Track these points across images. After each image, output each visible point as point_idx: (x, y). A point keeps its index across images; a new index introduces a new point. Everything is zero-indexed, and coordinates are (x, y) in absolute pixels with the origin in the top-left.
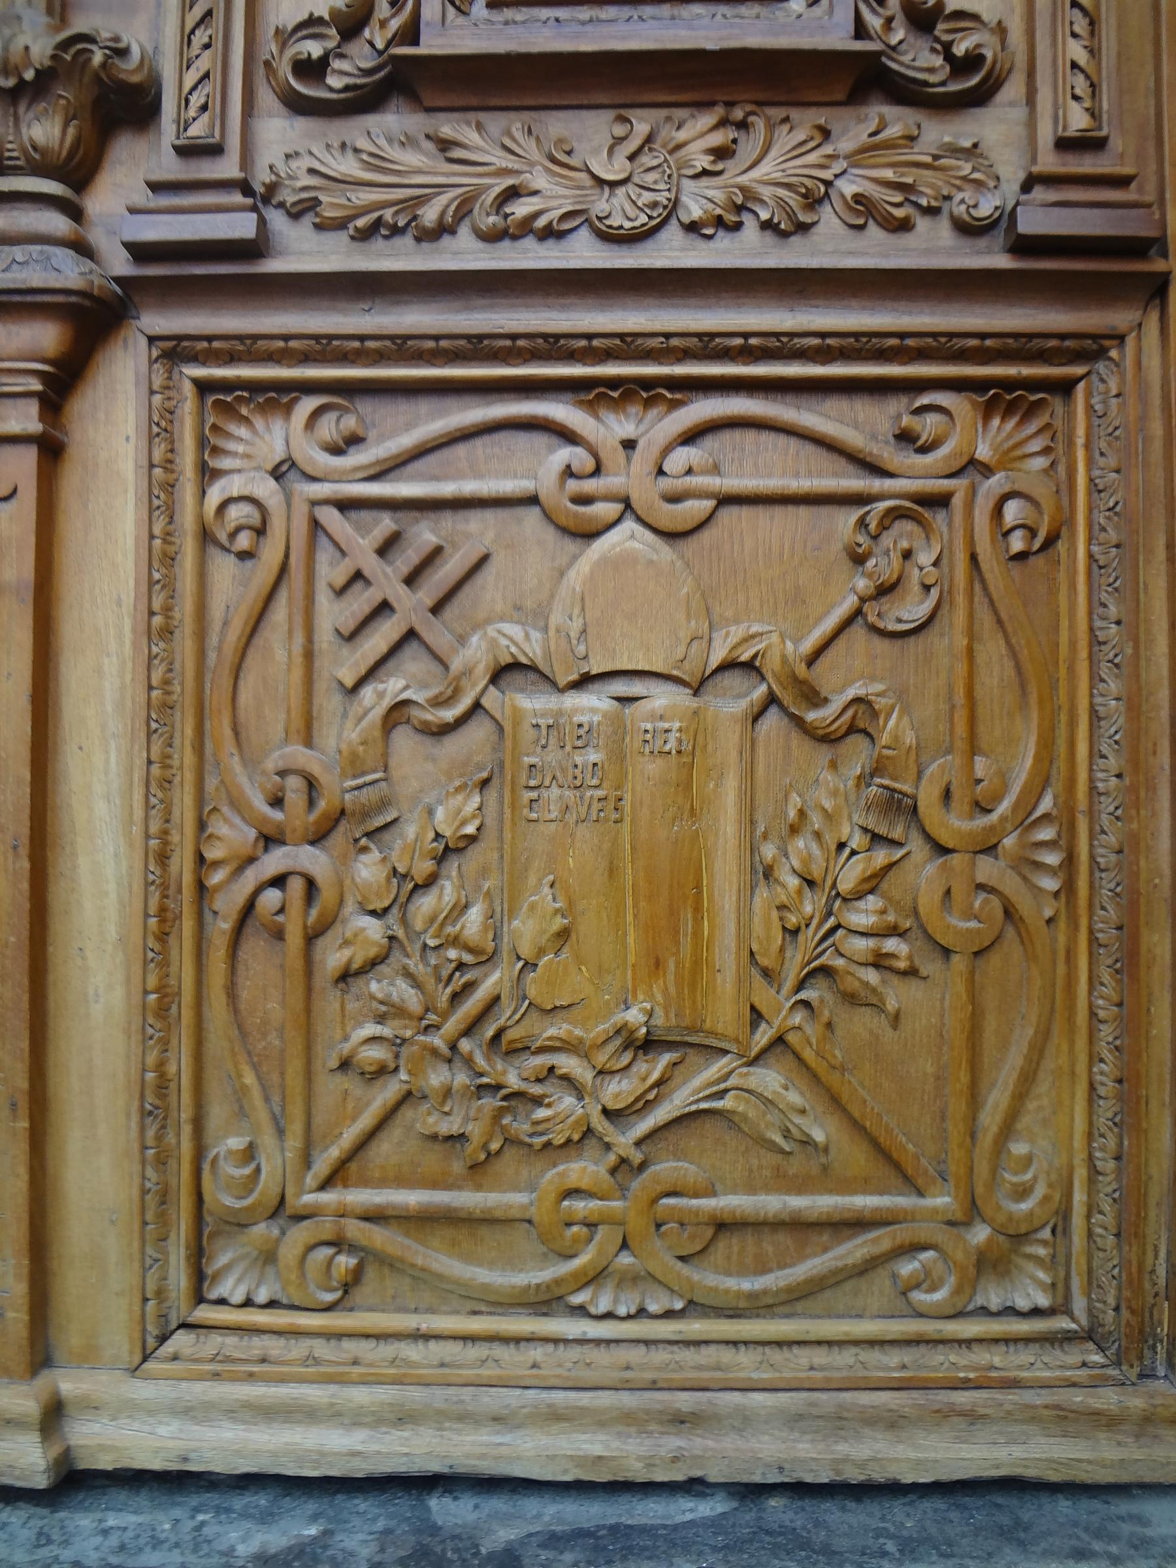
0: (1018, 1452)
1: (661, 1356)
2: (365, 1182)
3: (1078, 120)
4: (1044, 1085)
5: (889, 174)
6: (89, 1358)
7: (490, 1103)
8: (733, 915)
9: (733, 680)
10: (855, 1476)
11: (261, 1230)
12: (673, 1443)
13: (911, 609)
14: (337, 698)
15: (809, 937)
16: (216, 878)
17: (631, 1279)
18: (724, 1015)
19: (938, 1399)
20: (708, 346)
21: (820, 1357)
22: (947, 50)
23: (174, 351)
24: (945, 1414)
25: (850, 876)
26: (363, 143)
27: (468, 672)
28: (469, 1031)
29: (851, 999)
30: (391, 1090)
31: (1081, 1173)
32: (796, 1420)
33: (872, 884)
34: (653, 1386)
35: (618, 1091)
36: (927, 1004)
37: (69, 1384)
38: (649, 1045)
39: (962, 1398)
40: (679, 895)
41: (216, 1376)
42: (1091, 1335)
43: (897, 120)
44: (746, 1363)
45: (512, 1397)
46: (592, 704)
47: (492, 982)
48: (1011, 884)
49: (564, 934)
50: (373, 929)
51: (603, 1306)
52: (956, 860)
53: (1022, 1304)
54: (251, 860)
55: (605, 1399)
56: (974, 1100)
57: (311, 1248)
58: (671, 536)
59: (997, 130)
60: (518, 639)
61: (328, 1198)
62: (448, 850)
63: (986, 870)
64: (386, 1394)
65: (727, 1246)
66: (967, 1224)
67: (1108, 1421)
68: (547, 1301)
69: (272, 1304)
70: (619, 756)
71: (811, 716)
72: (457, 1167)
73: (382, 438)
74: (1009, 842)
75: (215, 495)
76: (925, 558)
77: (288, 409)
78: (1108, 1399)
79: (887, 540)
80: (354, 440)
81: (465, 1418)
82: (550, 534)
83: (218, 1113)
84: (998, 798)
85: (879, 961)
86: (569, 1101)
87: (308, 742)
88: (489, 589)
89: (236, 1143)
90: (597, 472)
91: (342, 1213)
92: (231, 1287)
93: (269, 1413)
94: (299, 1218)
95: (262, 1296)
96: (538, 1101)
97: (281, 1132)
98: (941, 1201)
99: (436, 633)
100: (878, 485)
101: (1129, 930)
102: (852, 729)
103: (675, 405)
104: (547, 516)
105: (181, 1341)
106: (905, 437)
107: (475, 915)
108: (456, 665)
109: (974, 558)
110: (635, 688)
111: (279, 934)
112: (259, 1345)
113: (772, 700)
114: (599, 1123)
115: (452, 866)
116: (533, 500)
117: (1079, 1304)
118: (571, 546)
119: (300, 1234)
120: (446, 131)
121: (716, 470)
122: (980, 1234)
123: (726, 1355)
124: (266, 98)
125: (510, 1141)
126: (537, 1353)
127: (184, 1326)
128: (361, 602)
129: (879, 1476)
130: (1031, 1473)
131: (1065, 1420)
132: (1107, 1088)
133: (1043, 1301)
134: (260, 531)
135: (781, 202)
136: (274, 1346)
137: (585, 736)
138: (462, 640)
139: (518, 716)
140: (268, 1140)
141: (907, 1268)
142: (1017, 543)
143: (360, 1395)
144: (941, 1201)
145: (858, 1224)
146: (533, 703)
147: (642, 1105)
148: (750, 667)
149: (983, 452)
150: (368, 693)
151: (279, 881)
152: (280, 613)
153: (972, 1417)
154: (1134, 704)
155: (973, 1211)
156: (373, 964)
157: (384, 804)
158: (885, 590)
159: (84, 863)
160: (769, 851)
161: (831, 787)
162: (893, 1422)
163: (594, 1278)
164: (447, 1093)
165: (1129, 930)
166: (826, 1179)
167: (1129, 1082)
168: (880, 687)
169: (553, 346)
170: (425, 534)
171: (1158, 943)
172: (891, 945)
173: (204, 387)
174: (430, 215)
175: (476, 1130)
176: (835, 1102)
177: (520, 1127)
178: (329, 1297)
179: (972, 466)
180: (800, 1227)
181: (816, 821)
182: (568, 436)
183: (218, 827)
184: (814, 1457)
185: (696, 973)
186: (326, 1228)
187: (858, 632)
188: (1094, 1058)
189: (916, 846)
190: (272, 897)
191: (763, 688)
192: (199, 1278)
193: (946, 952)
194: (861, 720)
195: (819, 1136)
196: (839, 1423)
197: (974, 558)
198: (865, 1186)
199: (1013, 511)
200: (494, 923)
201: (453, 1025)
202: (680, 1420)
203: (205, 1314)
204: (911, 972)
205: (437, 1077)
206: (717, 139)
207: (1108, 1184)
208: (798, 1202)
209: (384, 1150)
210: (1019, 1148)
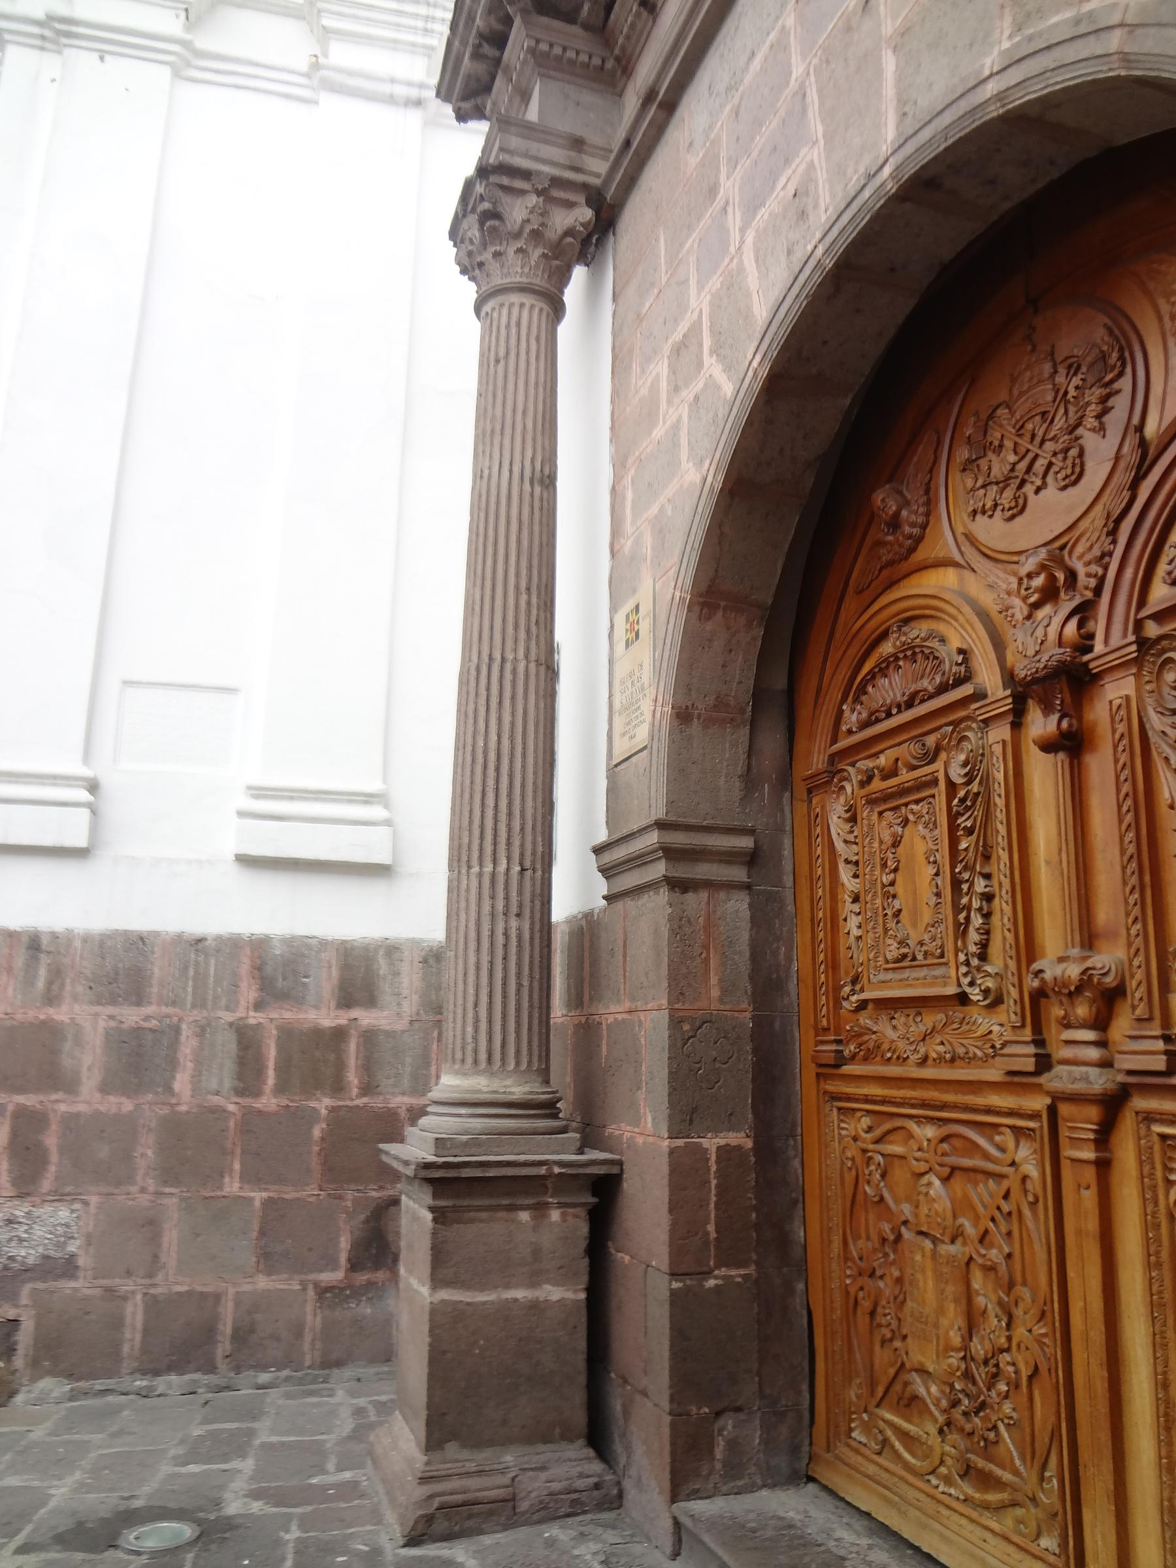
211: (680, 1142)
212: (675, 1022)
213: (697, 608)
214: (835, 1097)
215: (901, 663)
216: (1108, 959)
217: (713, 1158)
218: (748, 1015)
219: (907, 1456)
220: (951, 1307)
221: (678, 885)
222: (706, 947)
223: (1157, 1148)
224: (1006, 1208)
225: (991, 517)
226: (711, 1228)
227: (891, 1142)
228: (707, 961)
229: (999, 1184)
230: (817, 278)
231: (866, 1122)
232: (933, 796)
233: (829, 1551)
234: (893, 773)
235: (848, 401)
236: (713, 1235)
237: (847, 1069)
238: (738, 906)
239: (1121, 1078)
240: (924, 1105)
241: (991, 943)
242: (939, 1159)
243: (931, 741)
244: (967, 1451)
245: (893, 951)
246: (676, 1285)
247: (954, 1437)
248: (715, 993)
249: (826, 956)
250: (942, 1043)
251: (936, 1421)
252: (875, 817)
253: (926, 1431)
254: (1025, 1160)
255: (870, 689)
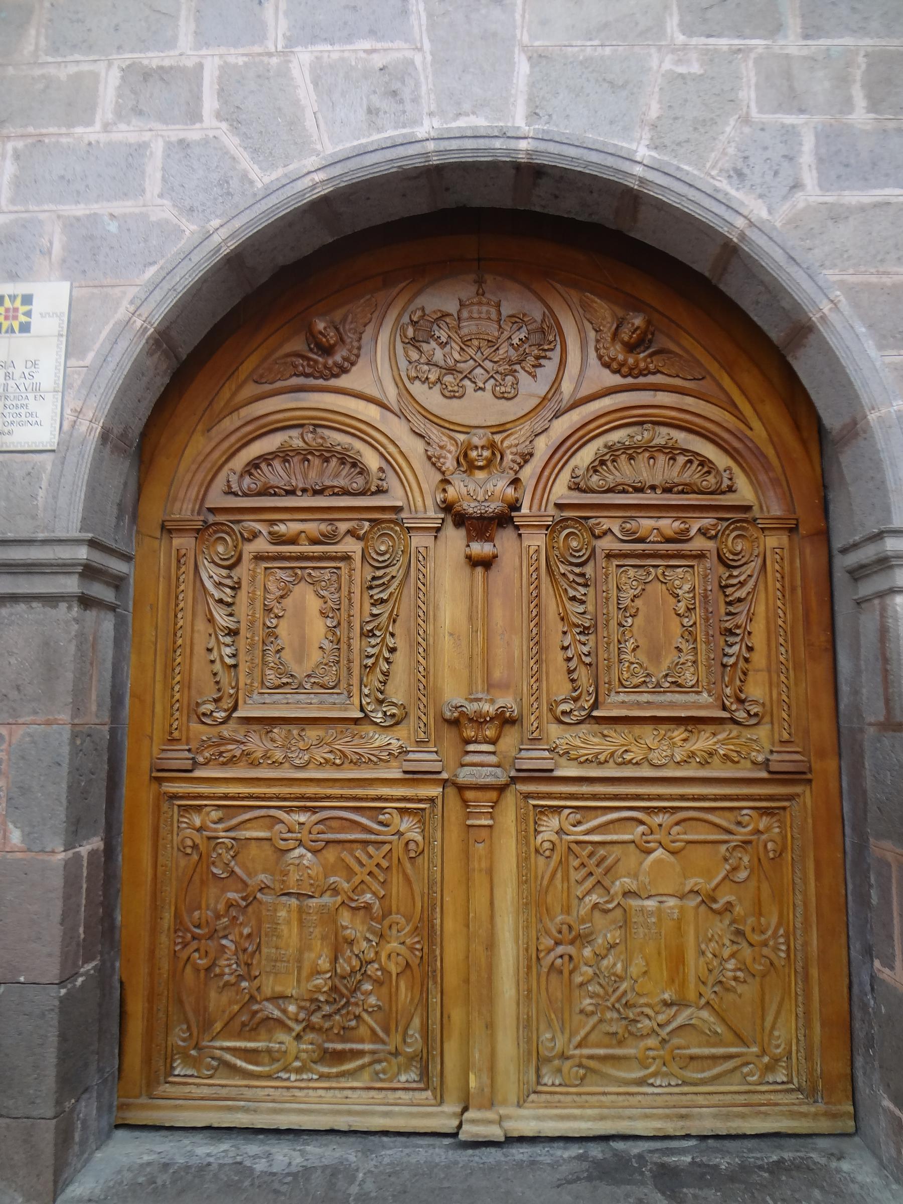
0: (779, 1124)
1: (675, 1098)
2: (587, 1047)
3: (786, 736)
4: (783, 1013)
5: (732, 747)
6: (504, 1103)
7: (624, 1022)
8: (693, 965)
9: (692, 895)
10: (733, 1132)
11: (556, 1062)
12: (681, 1123)
13: (742, 875)
14: (577, 901)
15: (716, 972)
16: (542, 955)
17: (666, 1075)
18: (692, 995)
19: (755, 1109)
20: (683, 798)
21: (721, 1097)
22: (748, 712)
23: (527, 796)
24: (759, 1113)
25: (726, 953)
26: (581, 735)
27: (616, 893)
28: (619, 1000)
29: (727, 990)
30: (595, 1019)
31: (794, 1041)
32: (715, 1116)
33: (733, 955)
34: (674, 1107)
35: (661, 1018)
36: (748, 991)
37: (502, 1111)
38: (667, 1004)
39: (763, 1109)
40: (677, 960)
41: (546, 1107)
42: (799, 1090)
43: (735, 731)
44: (700, 1100)
45: (634, 1111)
46: (651, 904)
47: (624, 986)
48: (773, 956)
49: (645, 973)
50: (590, 971)
51: (658, 1083)
52: (756, 949)
53: (779, 1080)
54: (553, 950)
55: (660, 1111)
56: (763, 1019)
57: (571, 1067)
58: (673, 853)
59: (762, 732)
60: (627, 882)
61: (577, 1052)
62: (612, 946)
63: (765, 951)
64: (596, 1111)
65: (694, 1064)
66: (762, 1056)
67: (804, 1115)
68: (641, 1082)
69: (560, 1085)
70: (660, 919)
71: (715, 906)
72: (614, 1042)
73: (587, 822)
74: (771, 943)
75: (539, 838)
76: (746, 859)
77: (560, 813)
78: (804, 1109)
79: (735, 854)
80: (579, 823)
81: (620, 1117)
82: (638, 852)
83: (542, 1026)
84: (767, 930)
85: (735, 979)
86: (647, 1022)
87: (568, 914)
88: (621, 868)
89: (548, 1036)
90: (652, 833)
91: (581, 1056)
92: (547, 1079)
93: (562, 1118)
94: (568, 1058)
95: (557, 1082)
96: (638, 1021)
97: (562, 1033)
98: (755, 1049)
99: (606, 882)
100: (731, 837)
101: (806, 968)
102: (726, 910)
103: (673, 814)
104: (637, 846)
105: (533, 1097)
106: (739, 823)
107: (619, 966)
108: (612, 892)
109: (759, 860)
110: (664, 898)
111: (561, 972)
112: (557, 1097)
113: (703, 901)
114: (656, 1027)
115: (612, 951)
116: (633, 842)
117: (795, 1080)
118: (644, 855)
119: (568, 1064)
120: (605, 732)
121: (685, 833)
122: (766, 1059)
123: (694, 1097)
124: (550, 715)
125: (631, 1034)
126: (639, 1098)
127: (535, 1092)
128: (583, 872)
129: (740, 1132)
130: (783, 1131)
131: (793, 1115)
132: (801, 1015)
133: (785, 1079)
134: (552, 850)
135: (703, 756)
136: (562, 1098)
137: (651, 914)
138: (613, 883)
139: (630, 906)
140: (559, 1034)
141: (745, 1070)
142: (771, 855)
143: (589, 1112)
144: (755, 1049)
145: (730, 1057)
146: (634, 903)
147: (669, 1022)
148: (697, 892)
149: (761, 827)
150: (587, 899)
151: (561, 957)
152: (559, 875)
153: (766, 1114)
154: (805, 904)
155: (764, 1052)
156: (589, 981)
157: (592, 933)
158: (735, 869)
159: (502, 951)
160: (703, 946)
161: (720, 927)
162: (743, 1116)
163: (655, 1075)
164: (612, 1020)
165: (806, 968)
166: (721, 1044)
167: (807, 1013)
168: (734, 898)
169: (638, 797)
170: (602, 852)
171: (814, 972)
172: (739, 974)
173: (534, 806)
174: (602, 758)
175: (620, 1031)
176: (723, 1020)
177: (633, 1029)
178: (578, 1082)
179: (758, 832)
180: (714, 1058)
181: (716, 937)
182: (642, 823)
183: (542, 940)
184: (722, 1127)
185: (683, 984)
186: (577, 1061)
187: (727, 881)
188: (797, 1006)
189: (745, 944)
190: (559, 961)
191: (700, 899)
192: (538, 1077)
193: (754, 976)
194: (729, 907)
195: (719, 1031)
196: (728, 1117)
197: (759, 860)
198: (732, 1045)
199: (770, 845)
200: (625, 969)
201: (613, 999)
202: (682, 1117)
203: (540, 1088)
204: (745, 982)
205: (609, 1015)
206: (684, 736)
207: (802, 1043)
208: (714, 1051)
209: (593, 1037)
210: (776, 1033)
211: (70, 853)
212: (74, 736)
213: (151, 342)
214: (175, 797)
215: (309, 457)
216: (506, 701)
217: (85, 864)
218: (107, 728)
219: (251, 1067)
220: (318, 944)
221: (86, 602)
222: (91, 664)
223: (531, 813)
224: (385, 864)
225: (430, 388)
226: (81, 930)
227: (246, 829)
228: (91, 676)
229: (377, 849)
230: (419, 162)
231: (215, 815)
232: (339, 568)
233: (221, 1166)
234: (293, 541)
235: (330, 240)
236: (82, 936)
237: (197, 774)
238: (108, 624)
239: (513, 773)
240: (303, 798)
241: (389, 682)
242: (313, 837)
243: (343, 527)
244: (324, 1042)
245: (271, 677)
246: (63, 991)
247: (310, 1036)
248: (94, 708)
249: (183, 678)
250: (331, 752)
251: (290, 1029)
252: (260, 570)
253: (284, 1040)
254: (410, 830)
255: (263, 466)
